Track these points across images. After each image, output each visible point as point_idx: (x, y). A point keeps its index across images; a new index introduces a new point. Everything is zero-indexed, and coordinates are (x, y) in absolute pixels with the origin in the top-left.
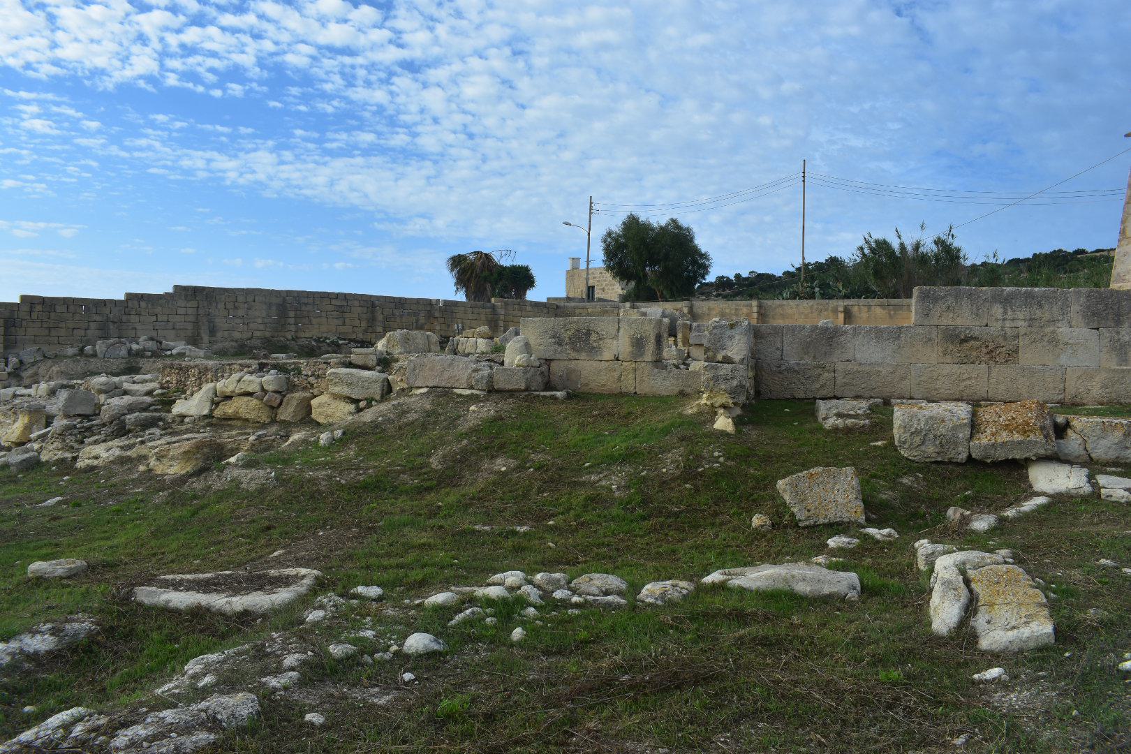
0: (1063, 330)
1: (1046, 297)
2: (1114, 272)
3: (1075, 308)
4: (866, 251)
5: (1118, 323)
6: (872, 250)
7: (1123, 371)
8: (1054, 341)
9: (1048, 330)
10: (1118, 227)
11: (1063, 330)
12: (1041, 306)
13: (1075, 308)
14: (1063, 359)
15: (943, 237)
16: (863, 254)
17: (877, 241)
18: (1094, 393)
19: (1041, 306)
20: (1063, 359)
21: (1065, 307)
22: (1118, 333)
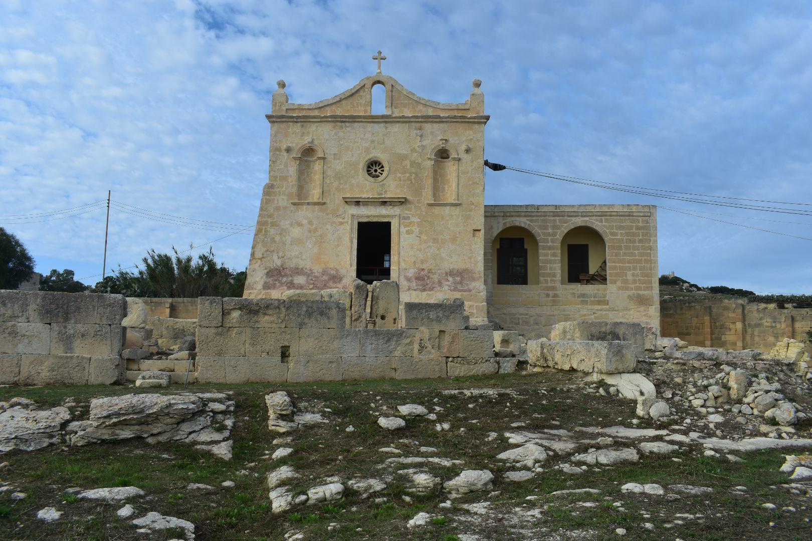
0: (22, 326)
1: (9, 298)
2: (247, 283)
3: (32, 307)
4: (150, 261)
5: (67, 319)
6: (154, 261)
7: (67, 357)
8: (14, 333)
9: (10, 324)
10: (249, 251)
11: (22, 326)
12: (5, 305)
13: (32, 307)
14: (21, 348)
15: (206, 255)
16: (148, 265)
17: (159, 256)
18: (43, 375)
19: (5, 305)
20: (21, 348)
21: (24, 307)
22: (65, 327)
